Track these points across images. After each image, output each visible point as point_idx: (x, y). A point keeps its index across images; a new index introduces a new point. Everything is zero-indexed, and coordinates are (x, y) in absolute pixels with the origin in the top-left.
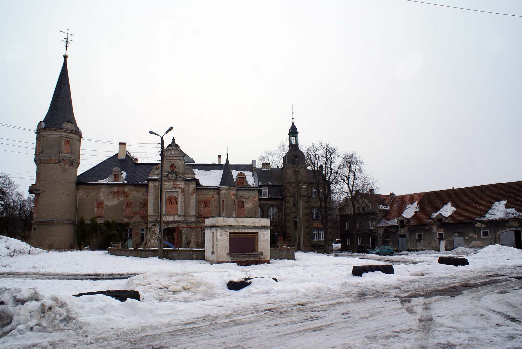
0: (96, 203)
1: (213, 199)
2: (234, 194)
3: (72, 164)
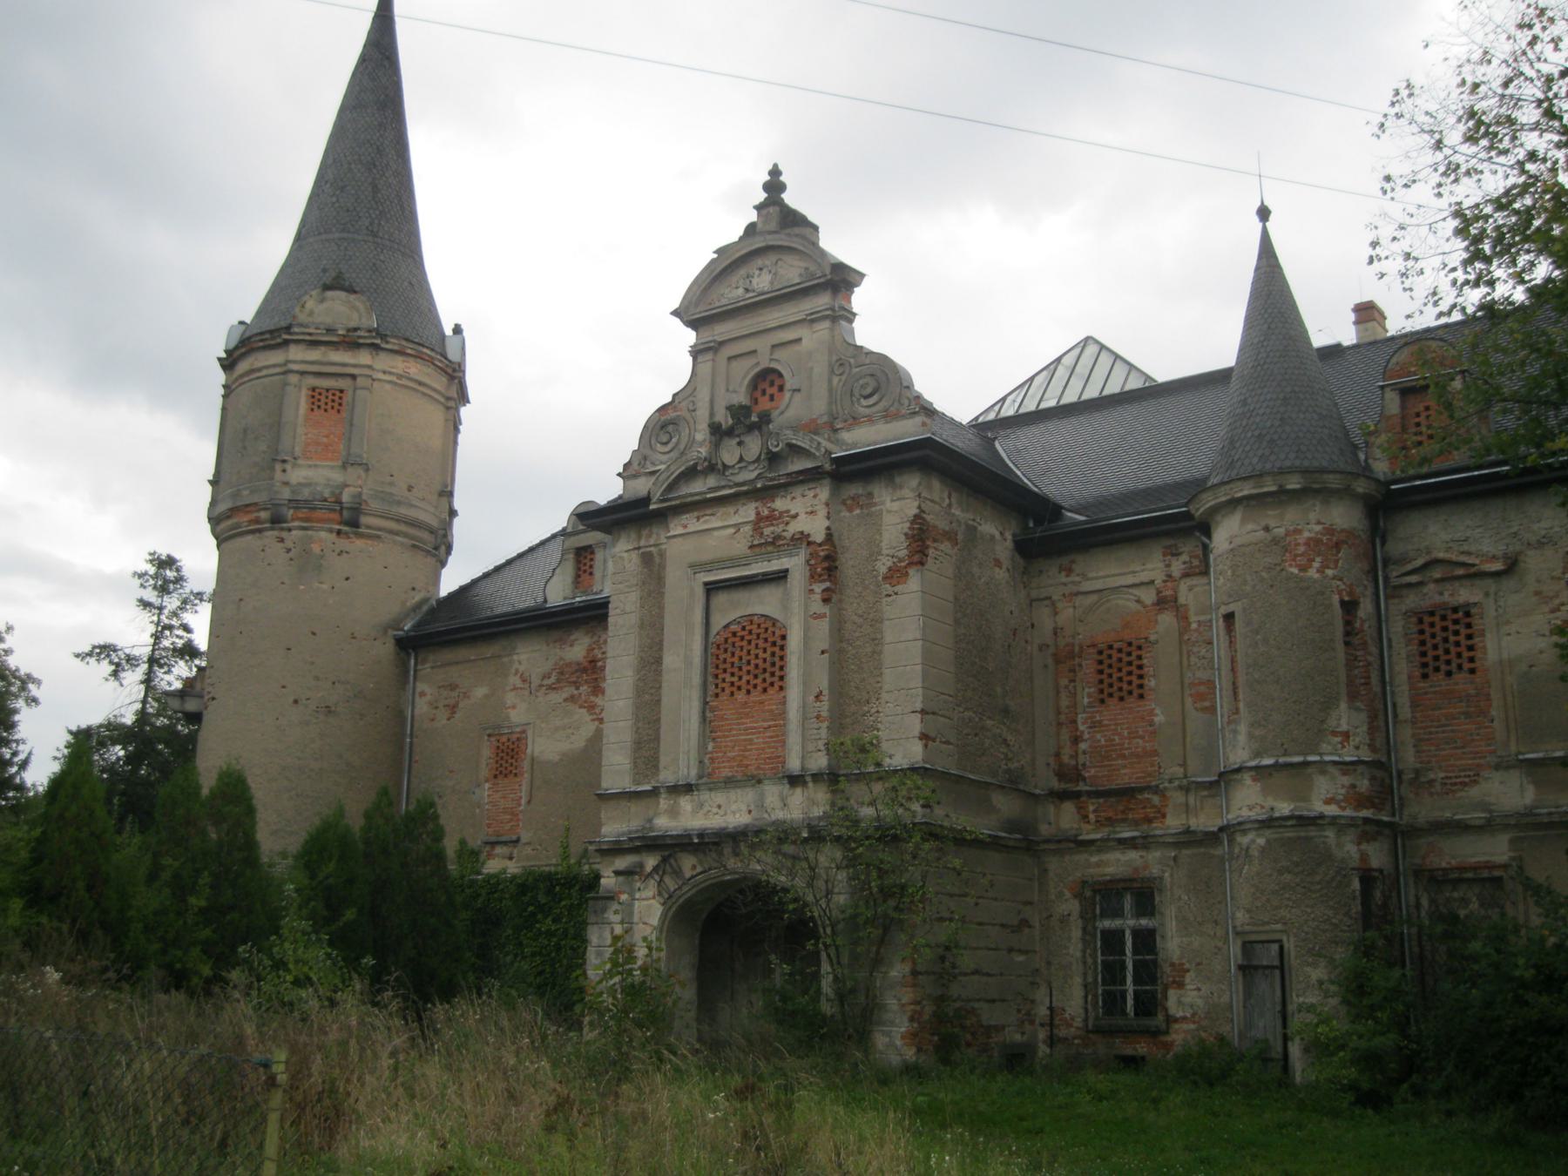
0: (487, 752)
1: (1167, 620)
2: (1329, 544)
3: (354, 524)
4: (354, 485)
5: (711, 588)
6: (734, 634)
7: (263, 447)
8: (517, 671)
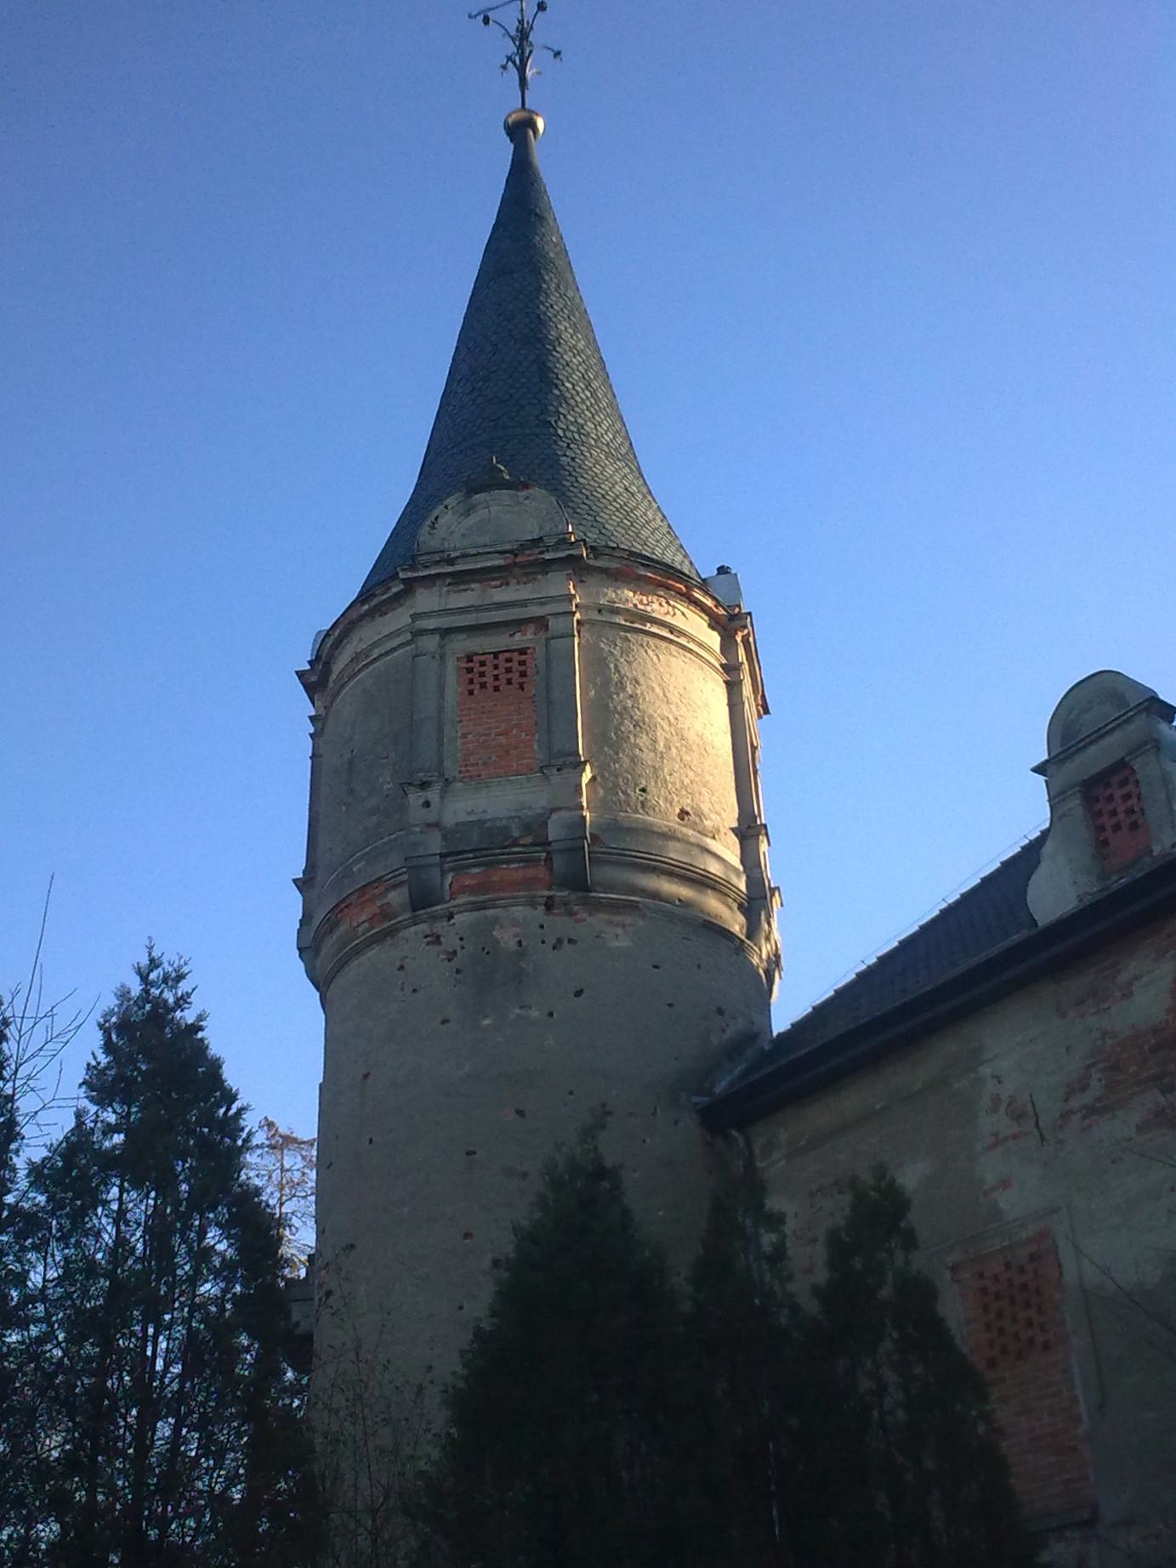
3: (579, 883)
8: (996, 1099)
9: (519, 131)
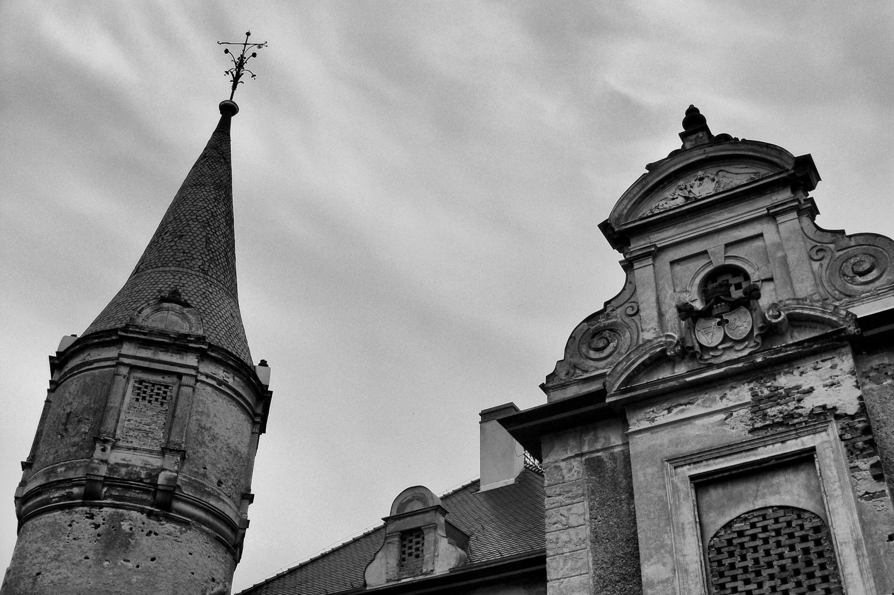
4: (168, 470)
5: (701, 483)
6: (741, 534)
7: (85, 428)
9: (228, 110)
